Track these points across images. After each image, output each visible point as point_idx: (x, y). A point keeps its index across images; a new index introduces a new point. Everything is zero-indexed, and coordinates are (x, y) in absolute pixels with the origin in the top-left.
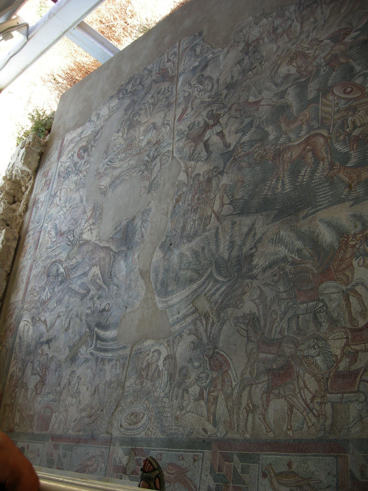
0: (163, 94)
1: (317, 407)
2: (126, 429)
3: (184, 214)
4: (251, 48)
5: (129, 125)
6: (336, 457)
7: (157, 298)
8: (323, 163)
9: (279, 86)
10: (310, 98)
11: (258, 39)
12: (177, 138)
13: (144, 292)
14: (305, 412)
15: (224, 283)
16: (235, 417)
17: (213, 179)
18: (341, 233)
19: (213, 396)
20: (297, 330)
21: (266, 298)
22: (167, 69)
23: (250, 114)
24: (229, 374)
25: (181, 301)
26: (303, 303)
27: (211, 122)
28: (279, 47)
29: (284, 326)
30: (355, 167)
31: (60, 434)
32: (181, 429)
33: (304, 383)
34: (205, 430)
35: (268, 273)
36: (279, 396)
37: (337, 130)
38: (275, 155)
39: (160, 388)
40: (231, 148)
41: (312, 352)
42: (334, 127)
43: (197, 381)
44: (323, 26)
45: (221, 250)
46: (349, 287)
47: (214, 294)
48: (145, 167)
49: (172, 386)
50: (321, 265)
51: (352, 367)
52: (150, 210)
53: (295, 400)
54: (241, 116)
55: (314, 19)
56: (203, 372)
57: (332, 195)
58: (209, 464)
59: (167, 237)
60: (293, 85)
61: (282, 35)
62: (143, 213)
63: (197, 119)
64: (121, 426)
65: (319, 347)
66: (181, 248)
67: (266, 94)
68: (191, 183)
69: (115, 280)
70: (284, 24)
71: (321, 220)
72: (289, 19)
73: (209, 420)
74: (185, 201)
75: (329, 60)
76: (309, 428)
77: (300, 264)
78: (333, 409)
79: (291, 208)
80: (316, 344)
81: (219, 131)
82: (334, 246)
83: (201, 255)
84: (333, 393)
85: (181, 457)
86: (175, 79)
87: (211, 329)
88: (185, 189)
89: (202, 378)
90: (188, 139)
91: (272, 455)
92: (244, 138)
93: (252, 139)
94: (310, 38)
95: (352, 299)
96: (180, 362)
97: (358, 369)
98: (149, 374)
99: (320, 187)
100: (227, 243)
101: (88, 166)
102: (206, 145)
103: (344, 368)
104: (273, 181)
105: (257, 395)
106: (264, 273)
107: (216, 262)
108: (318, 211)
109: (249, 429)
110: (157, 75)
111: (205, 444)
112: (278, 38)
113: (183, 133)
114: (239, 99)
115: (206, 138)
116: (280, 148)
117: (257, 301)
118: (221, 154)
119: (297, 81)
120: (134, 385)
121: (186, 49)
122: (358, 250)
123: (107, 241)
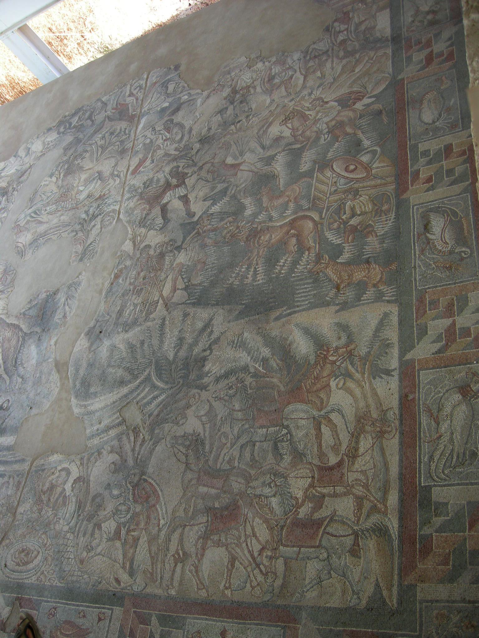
0: (117, 136)
1: (266, 562)
2: (11, 570)
3: (123, 295)
4: (238, 96)
5: (67, 169)
6: (284, 628)
7: (74, 401)
8: (309, 253)
9: (266, 150)
10: (303, 170)
11: (248, 87)
12: (127, 196)
13: (57, 390)
14: (250, 567)
15: (163, 390)
16: (159, 566)
17: (167, 254)
18: (320, 344)
19: (133, 536)
20: (251, 461)
21: (216, 415)
22: (128, 104)
23: (225, 179)
24: (157, 509)
25: (104, 408)
26: (262, 427)
27: (174, 181)
28: (274, 100)
29: (234, 454)
30: (348, 263)
32: (86, 576)
33: (253, 529)
34: (118, 581)
35: (223, 384)
36: (218, 544)
37: (331, 215)
38: (249, 235)
39: (64, 519)
40: (195, 219)
41: (267, 491)
42: (328, 210)
43: (114, 514)
44: (332, 84)
45: (165, 347)
46: (322, 413)
47: (149, 403)
48: (80, 226)
49: (81, 518)
50: (290, 381)
51: (315, 514)
52: (79, 284)
53: (238, 550)
54: (214, 179)
55: (321, 73)
56: (124, 504)
57: (314, 295)
58: (118, 625)
59: (97, 322)
60: (284, 150)
61: (279, 86)
63: (156, 175)
64: (6, 566)
65: (276, 485)
66: (114, 339)
67: (248, 157)
68: (138, 256)
69: (21, 369)
70: (284, 74)
71: (297, 325)
72: (290, 68)
73: (124, 567)
74: (126, 278)
75: (333, 127)
76: (253, 588)
77: (264, 377)
78: (285, 567)
79: (260, 305)
80: (273, 481)
81: (182, 194)
82: (309, 360)
83: (138, 350)
84: (287, 546)
85: (82, 614)
86: (136, 119)
87: (140, 448)
88: (128, 263)
89: (121, 511)
90: (141, 198)
91: (202, 619)
92: (213, 208)
93: (224, 210)
94: (313, 96)
95: (325, 429)
96: (94, 488)
97: (323, 518)
99: (300, 282)
100: (175, 339)
101: (5, 215)
102: (164, 210)
103: (305, 515)
104: (243, 268)
105: (191, 541)
106: (217, 383)
107: (157, 362)
108: (295, 312)
109: (176, 584)
110: (114, 111)
111: (116, 598)
112: (273, 90)
113: (136, 190)
114: (214, 158)
115: (165, 201)
116: (257, 228)
117: (204, 418)
118: (181, 225)
119: (290, 147)
120: (29, 513)
121: (155, 83)
122: (339, 368)
123: (16, 317)
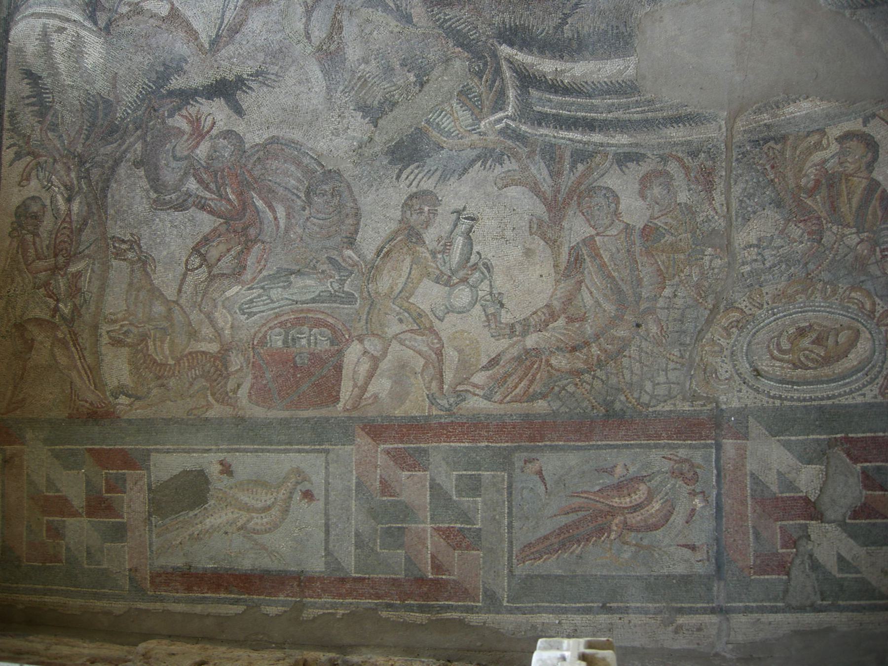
31: (415, 413)
64: (758, 373)
98: (844, 209)
120: (778, 242)
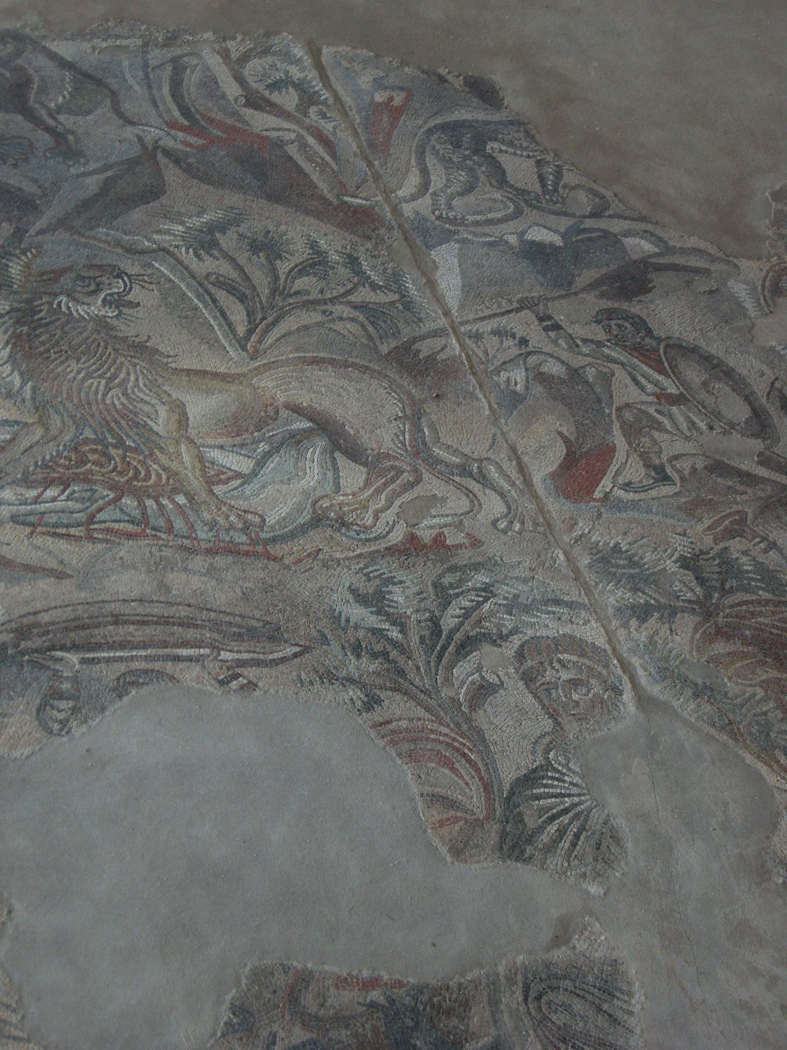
62: (541, 986)
